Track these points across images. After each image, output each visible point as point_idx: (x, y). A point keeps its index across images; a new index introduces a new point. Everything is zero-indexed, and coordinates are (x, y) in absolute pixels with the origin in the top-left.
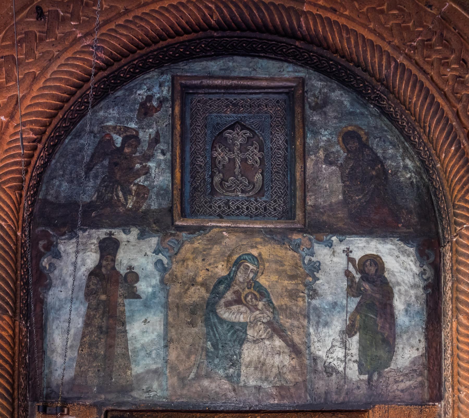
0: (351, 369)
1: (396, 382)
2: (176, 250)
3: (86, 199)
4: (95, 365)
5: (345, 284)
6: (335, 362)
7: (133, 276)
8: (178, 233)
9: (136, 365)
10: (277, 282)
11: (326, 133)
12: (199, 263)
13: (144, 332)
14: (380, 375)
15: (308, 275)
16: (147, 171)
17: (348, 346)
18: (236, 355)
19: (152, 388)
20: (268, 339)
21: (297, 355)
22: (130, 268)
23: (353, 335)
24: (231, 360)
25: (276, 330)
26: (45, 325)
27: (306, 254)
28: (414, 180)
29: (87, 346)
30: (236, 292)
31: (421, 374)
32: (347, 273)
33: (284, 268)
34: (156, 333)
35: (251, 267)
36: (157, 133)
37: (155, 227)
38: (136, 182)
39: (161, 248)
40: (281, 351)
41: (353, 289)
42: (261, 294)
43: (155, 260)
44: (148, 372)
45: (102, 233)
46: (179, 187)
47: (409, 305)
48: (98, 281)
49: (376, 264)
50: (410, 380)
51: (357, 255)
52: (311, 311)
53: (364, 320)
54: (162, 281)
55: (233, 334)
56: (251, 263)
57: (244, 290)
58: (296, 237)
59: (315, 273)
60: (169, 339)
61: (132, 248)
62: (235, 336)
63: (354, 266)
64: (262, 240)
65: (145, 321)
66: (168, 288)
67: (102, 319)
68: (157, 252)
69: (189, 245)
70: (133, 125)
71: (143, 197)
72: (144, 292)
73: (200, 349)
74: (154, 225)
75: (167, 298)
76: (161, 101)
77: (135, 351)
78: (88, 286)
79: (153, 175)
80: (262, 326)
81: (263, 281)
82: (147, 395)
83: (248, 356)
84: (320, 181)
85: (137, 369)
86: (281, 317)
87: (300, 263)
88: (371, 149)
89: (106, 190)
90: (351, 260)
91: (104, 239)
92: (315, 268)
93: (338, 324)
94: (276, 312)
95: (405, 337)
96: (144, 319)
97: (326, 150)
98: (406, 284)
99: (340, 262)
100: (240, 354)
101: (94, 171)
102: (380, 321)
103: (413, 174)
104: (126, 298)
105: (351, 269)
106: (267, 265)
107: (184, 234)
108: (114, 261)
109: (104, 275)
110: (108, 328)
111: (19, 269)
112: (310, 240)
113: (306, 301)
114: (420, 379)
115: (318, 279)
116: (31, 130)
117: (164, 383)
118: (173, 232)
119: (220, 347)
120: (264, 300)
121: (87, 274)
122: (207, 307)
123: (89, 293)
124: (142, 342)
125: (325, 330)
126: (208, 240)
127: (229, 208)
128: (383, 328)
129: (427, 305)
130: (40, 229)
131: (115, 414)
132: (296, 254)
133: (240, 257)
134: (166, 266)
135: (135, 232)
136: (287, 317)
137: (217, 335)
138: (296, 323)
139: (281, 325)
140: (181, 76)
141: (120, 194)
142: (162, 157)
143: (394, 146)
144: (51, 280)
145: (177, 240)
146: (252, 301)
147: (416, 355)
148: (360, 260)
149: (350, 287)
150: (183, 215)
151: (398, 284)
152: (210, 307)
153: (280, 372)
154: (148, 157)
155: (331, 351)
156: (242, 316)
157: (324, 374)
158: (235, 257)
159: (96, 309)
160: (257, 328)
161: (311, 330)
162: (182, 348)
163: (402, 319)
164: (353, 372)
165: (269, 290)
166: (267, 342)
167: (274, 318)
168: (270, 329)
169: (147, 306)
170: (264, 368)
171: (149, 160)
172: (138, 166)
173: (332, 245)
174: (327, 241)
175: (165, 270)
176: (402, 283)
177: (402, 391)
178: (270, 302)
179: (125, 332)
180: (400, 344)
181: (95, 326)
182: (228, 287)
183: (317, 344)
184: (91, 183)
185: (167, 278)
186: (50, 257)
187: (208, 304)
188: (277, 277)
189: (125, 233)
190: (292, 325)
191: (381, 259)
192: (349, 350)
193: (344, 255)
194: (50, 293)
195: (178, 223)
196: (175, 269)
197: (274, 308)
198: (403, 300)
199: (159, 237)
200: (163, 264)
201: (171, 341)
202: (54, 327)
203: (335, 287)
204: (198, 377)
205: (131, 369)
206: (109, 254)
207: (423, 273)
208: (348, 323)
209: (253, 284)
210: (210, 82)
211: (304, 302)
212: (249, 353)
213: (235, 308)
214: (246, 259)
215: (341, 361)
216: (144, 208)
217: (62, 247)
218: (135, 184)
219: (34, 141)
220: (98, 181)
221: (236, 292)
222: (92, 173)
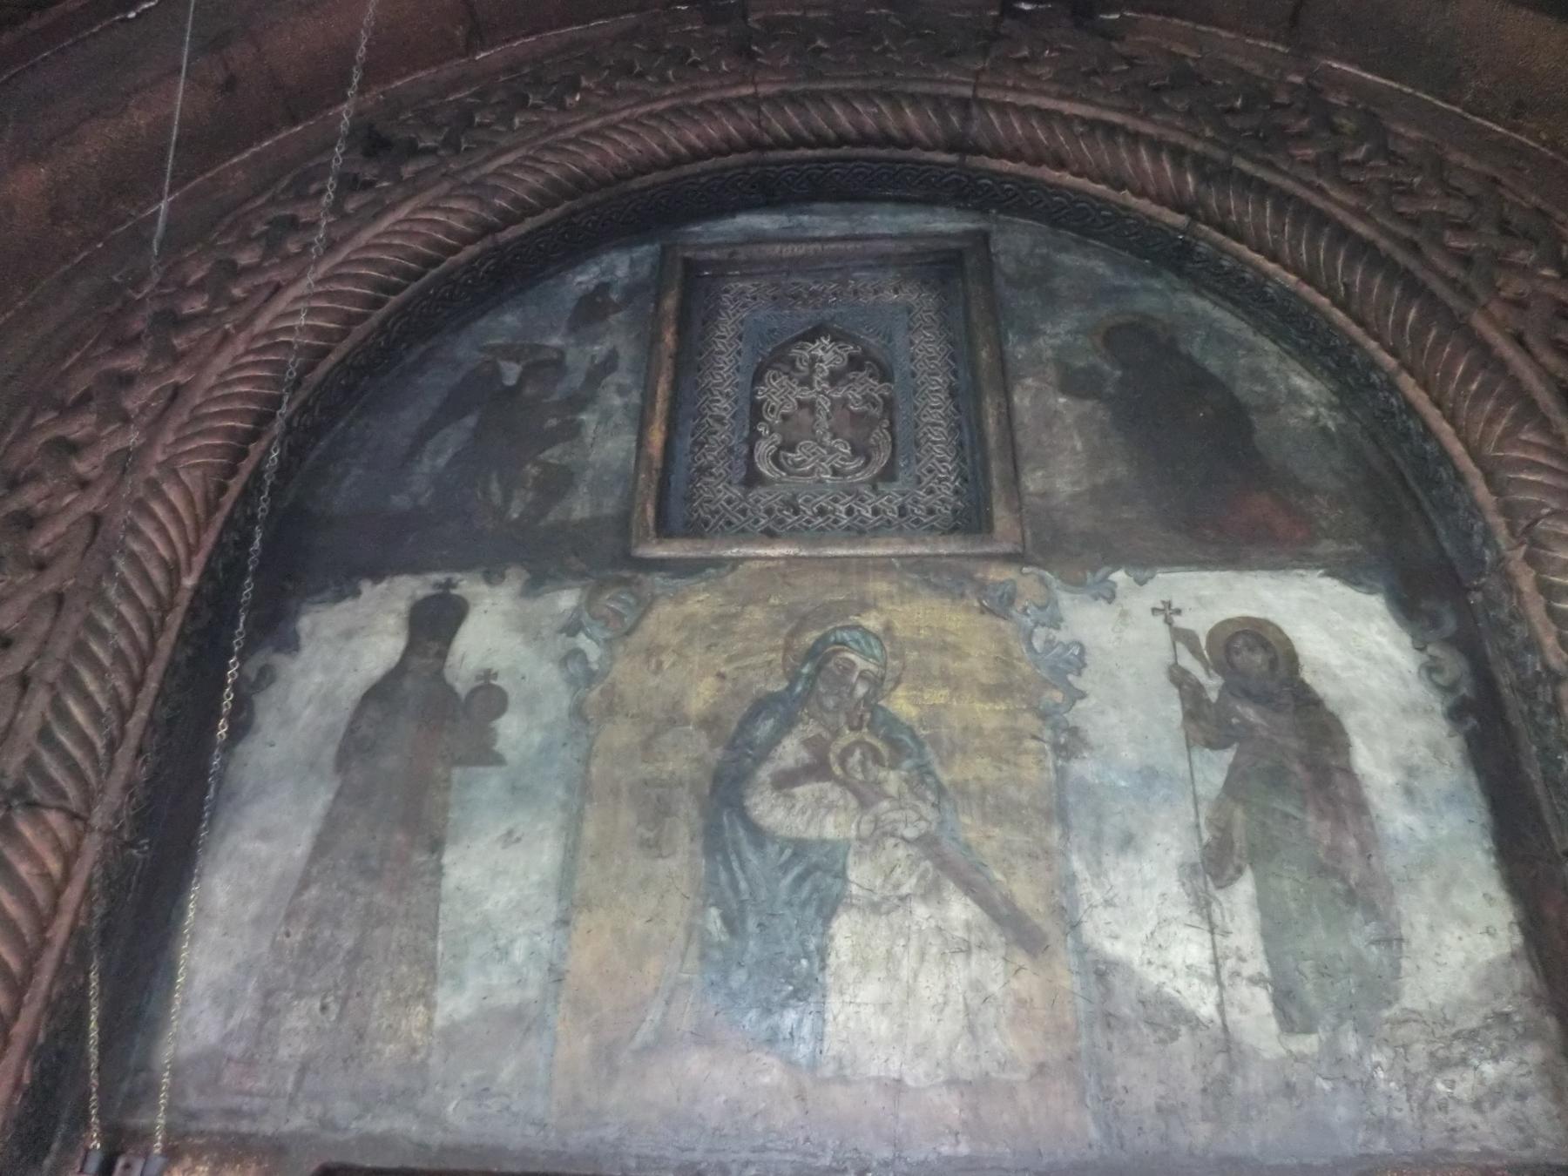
0: (1244, 1010)
3: (400, 501)
5: (1174, 710)
6: (1181, 984)
7: (490, 697)
8: (641, 576)
10: (945, 706)
15: (1046, 684)
16: (572, 431)
17: (1217, 917)
18: (808, 956)
20: (924, 898)
23: (1233, 880)
24: (789, 977)
25: (951, 867)
27: (1037, 623)
28: (1331, 424)
32: (1178, 677)
33: (965, 665)
34: (535, 877)
35: (861, 664)
40: (974, 940)
41: (1205, 723)
42: (895, 745)
47: (1411, 771)
49: (1266, 646)
51: (1200, 622)
52: (1071, 799)
55: (801, 879)
56: (862, 653)
57: (836, 734)
58: (997, 574)
59: (1071, 677)
62: (807, 888)
63: (1195, 651)
64: (894, 589)
69: (669, 608)
70: (555, 341)
73: (681, 935)
74: (573, 559)
78: (351, 729)
79: (589, 440)
80: (901, 852)
81: (901, 704)
86: (966, 820)
87: (1020, 649)
90: (1182, 637)
91: (427, 600)
93: (1170, 844)
94: (946, 805)
95: (1427, 884)
96: (503, 829)
100: (823, 953)
103: (1322, 410)
105: (1187, 661)
106: (913, 656)
107: (658, 579)
108: (442, 655)
112: (1042, 580)
113: (1050, 764)
115: (1083, 695)
119: (751, 925)
120: (907, 764)
121: (358, 694)
122: (713, 791)
125: (1129, 863)
132: (1002, 623)
134: (595, 667)
137: (743, 885)
138: (1019, 839)
139: (968, 847)
141: (495, 487)
142: (617, 401)
148: (1212, 635)
152: (726, 790)
156: (830, 820)
157: (1146, 1030)
158: (810, 637)
160: (883, 860)
161: (1077, 864)
166: (921, 911)
167: (941, 823)
168: (928, 864)
171: (582, 409)
172: (553, 422)
175: (591, 677)
178: (924, 771)
179: (439, 871)
182: (787, 724)
185: (592, 703)
188: (945, 692)
191: (1280, 631)
192: (1226, 934)
193: (1159, 620)
197: (940, 790)
199: (583, 587)
201: (586, 904)
204: (663, 1042)
205: (431, 1006)
207: (1431, 669)
208: (1206, 836)
209: (868, 716)
211: (1043, 769)
213: (804, 791)
214: (844, 643)
215: (1202, 977)
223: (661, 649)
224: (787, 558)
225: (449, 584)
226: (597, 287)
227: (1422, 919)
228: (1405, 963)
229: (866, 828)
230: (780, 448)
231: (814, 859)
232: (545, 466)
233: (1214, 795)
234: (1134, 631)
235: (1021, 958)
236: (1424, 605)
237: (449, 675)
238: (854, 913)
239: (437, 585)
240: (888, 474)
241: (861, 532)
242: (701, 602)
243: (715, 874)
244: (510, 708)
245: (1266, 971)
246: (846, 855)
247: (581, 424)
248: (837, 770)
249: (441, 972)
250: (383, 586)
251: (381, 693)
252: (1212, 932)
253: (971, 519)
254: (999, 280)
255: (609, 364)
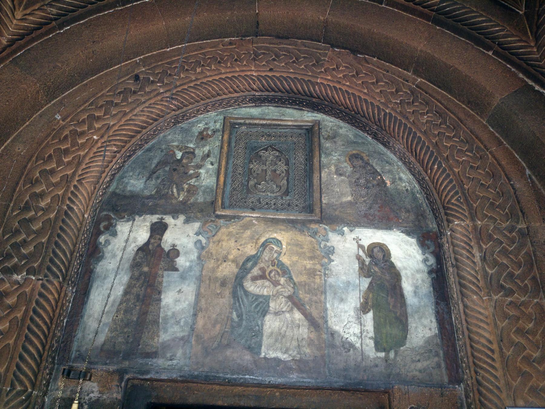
0: (367, 346)
1: (413, 361)
2: (214, 233)
4: (126, 330)
5: (356, 266)
7: (175, 252)
9: (164, 332)
10: (297, 261)
11: (336, 154)
12: (232, 243)
13: (177, 301)
14: (396, 353)
16: (198, 176)
17: (362, 322)
19: (175, 356)
21: (315, 328)
22: (174, 245)
23: (367, 312)
26: (89, 292)
27: (322, 240)
28: (409, 188)
29: (122, 312)
30: (263, 270)
31: (437, 355)
32: (358, 258)
34: (187, 303)
35: (276, 248)
36: (209, 151)
37: (199, 215)
38: (188, 182)
39: (201, 231)
40: (301, 324)
41: (364, 271)
43: (195, 240)
44: (173, 340)
45: (155, 218)
46: (222, 187)
47: (417, 287)
48: (144, 256)
50: (426, 360)
51: (366, 243)
52: (328, 288)
53: (377, 299)
54: (199, 258)
56: (275, 245)
57: (268, 267)
58: (313, 226)
59: (330, 256)
60: (198, 308)
61: (178, 230)
63: (364, 251)
65: (180, 291)
66: (203, 263)
67: (141, 288)
68: (197, 234)
69: (225, 230)
70: (191, 145)
71: (193, 193)
72: (182, 266)
73: (226, 319)
75: (202, 272)
76: (214, 132)
77: (166, 319)
78: (134, 259)
79: (202, 178)
80: (283, 300)
81: (285, 260)
82: (170, 363)
83: (270, 327)
84: (332, 186)
85: (164, 337)
86: (301, 292)
87: (317, 247)
88: (372, 166)
89: (164, 187)
90: (360, 246)
91: (156, 223)
92: (331, 251)
94: (296, 288)
96: (178, 289)
97: (336, 166)
98: (412, 269)
99: (352, 247)
100: (262, 325)
101: (157, 174)
102: (391, 300)
104: (165, 270)
107: (222, 221)
108: (160, 240)
109: (150, 251)
110: (145, 296)
111: (79, 243)
113: (323, 279)
114: (436, 359)
115: (333, 261)
116: (115, 145)
117: (188, 352)
118: (213, 219)
120: (286, 276)
121: (136, 249)
122: (235, 280)
123: (135, 265)
124: (173, 310)
125: (341, 306)
126: (241, 226)
127: (260, 203)
128: (394, 306)
129: (433, 288)
130: (105, 213)
131: (136, 382)
132: (313, 240)
133: (267, 240)
134: (204, 245)
135: (182, 218)
136: (306, 293)
139: (300, 299)
140: (230, 117)
141: (175, 190)
142: (211, 167)
143: (390, 164)
144: (103, 253)
145: (216, 226)
146: (275, 277)
147: (429, 335)
148: (369, 246)
149: (361, 269)
150: (223, 207)
151: (405, 268)
153: (299, 345)
154: (199, 167)
155: (348, 326)
156: (266, 290)
159: (138, 279)
160: (279, 301)
162: (209, 317)
163: (411, 299)
164: (369, 347)
165: (290, 268)
166: (288, 315)
168: (290, 303)
169: (183, 278)
170: (284, 340)
171: (200, 168)
172: (191, 172)
173: (343, 234)
174: (339, 230)
175: (203, 248)
176: (408, 268)
177: (420, 371)
178: (291, 278)
179: (160, 300)
180: (412, 324)
181: (133, 294)
182: (255, 264)
183: (333, 319)
184: (154, 182)
186: (108, 235)
187: (237, 277)
188: (297, 257)
189: (173, 218)
190: (310, 300)
192: (365, 326)
193: (355, 242)
194: (100, 264)
195: (218, 213)
196: (211, 248)
197: (295, 284)
198: (411, 282)
200: (201, 243)
201: (201, 310)
202: (96, 294)
203: (348, 268)
205: (158, 336)
206: (158, 234)
207: (425, 261)
208: (362, 300)
209: (276, 263)
210: (251, 121)
212: (271, 324)
213: (259, 282)
214: (271, 242)
216: (192, 200)
217: (119, 228)
218: (187, 184)
219: (115, 152)
220: (159, 181)
221: (263, 270)
222: (155, 176)
223: (222, 241)
224: (257, 217)
225: (162, 219)
226: (204, 128)
227: (414, 325)
228: (408, 336)
229: (275, 293)
230: (256, 183)
231: (261, 300)
232: (190, 184)
233: (365, 289)
234: (348, 244)
235: (312, 329)
236: (426, 242)
237: (162, 246)
238: (272, 316)
239: (158, 218)
240: (287, 193)
241: (277, 210)
242: (233, 228)
243: (235, 303)
244: (180, 255)
245: (374, 336)
246: (269, 299)
247: (200, 173)
248: (268, 277)
249: (161, 327)
250: (142, 217)
251: (143, 249)
252: (361, 325)
253: (309, 209)
254: (321, 138)
255: (208, 156)
